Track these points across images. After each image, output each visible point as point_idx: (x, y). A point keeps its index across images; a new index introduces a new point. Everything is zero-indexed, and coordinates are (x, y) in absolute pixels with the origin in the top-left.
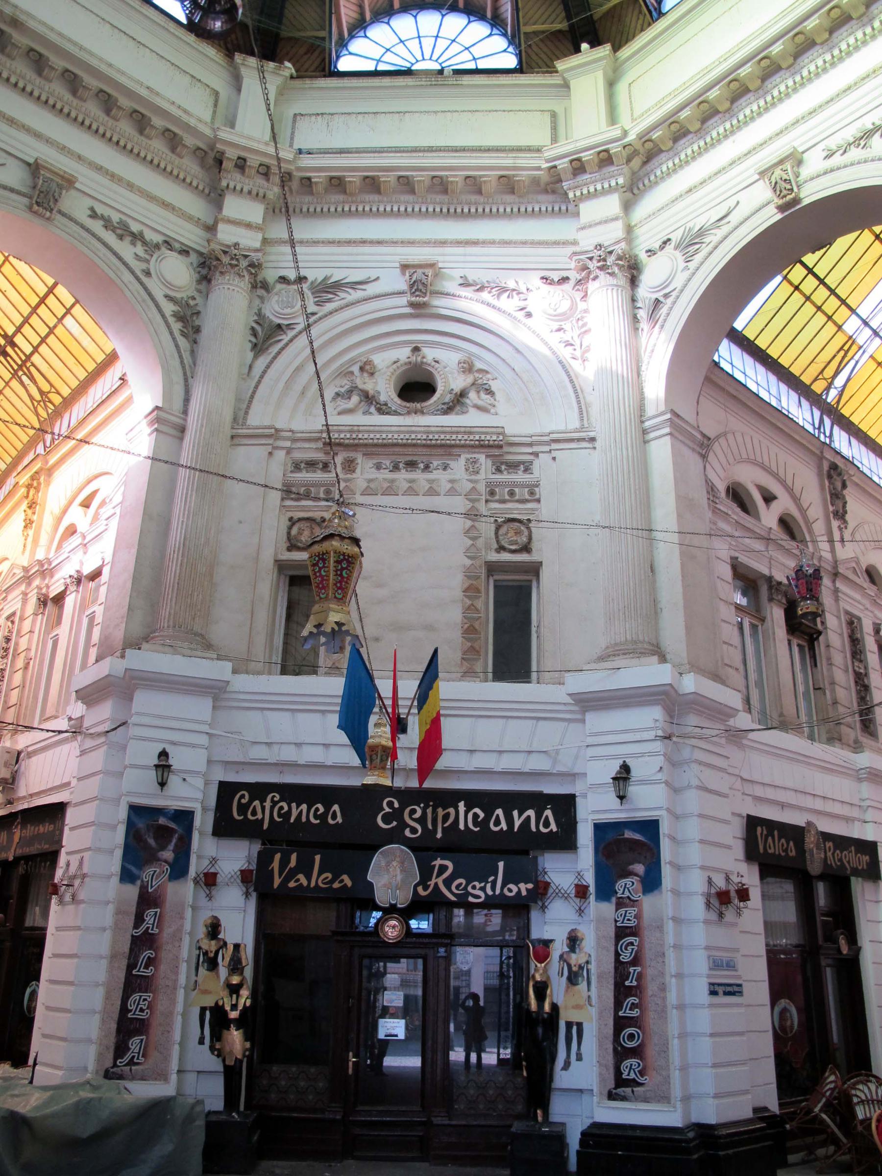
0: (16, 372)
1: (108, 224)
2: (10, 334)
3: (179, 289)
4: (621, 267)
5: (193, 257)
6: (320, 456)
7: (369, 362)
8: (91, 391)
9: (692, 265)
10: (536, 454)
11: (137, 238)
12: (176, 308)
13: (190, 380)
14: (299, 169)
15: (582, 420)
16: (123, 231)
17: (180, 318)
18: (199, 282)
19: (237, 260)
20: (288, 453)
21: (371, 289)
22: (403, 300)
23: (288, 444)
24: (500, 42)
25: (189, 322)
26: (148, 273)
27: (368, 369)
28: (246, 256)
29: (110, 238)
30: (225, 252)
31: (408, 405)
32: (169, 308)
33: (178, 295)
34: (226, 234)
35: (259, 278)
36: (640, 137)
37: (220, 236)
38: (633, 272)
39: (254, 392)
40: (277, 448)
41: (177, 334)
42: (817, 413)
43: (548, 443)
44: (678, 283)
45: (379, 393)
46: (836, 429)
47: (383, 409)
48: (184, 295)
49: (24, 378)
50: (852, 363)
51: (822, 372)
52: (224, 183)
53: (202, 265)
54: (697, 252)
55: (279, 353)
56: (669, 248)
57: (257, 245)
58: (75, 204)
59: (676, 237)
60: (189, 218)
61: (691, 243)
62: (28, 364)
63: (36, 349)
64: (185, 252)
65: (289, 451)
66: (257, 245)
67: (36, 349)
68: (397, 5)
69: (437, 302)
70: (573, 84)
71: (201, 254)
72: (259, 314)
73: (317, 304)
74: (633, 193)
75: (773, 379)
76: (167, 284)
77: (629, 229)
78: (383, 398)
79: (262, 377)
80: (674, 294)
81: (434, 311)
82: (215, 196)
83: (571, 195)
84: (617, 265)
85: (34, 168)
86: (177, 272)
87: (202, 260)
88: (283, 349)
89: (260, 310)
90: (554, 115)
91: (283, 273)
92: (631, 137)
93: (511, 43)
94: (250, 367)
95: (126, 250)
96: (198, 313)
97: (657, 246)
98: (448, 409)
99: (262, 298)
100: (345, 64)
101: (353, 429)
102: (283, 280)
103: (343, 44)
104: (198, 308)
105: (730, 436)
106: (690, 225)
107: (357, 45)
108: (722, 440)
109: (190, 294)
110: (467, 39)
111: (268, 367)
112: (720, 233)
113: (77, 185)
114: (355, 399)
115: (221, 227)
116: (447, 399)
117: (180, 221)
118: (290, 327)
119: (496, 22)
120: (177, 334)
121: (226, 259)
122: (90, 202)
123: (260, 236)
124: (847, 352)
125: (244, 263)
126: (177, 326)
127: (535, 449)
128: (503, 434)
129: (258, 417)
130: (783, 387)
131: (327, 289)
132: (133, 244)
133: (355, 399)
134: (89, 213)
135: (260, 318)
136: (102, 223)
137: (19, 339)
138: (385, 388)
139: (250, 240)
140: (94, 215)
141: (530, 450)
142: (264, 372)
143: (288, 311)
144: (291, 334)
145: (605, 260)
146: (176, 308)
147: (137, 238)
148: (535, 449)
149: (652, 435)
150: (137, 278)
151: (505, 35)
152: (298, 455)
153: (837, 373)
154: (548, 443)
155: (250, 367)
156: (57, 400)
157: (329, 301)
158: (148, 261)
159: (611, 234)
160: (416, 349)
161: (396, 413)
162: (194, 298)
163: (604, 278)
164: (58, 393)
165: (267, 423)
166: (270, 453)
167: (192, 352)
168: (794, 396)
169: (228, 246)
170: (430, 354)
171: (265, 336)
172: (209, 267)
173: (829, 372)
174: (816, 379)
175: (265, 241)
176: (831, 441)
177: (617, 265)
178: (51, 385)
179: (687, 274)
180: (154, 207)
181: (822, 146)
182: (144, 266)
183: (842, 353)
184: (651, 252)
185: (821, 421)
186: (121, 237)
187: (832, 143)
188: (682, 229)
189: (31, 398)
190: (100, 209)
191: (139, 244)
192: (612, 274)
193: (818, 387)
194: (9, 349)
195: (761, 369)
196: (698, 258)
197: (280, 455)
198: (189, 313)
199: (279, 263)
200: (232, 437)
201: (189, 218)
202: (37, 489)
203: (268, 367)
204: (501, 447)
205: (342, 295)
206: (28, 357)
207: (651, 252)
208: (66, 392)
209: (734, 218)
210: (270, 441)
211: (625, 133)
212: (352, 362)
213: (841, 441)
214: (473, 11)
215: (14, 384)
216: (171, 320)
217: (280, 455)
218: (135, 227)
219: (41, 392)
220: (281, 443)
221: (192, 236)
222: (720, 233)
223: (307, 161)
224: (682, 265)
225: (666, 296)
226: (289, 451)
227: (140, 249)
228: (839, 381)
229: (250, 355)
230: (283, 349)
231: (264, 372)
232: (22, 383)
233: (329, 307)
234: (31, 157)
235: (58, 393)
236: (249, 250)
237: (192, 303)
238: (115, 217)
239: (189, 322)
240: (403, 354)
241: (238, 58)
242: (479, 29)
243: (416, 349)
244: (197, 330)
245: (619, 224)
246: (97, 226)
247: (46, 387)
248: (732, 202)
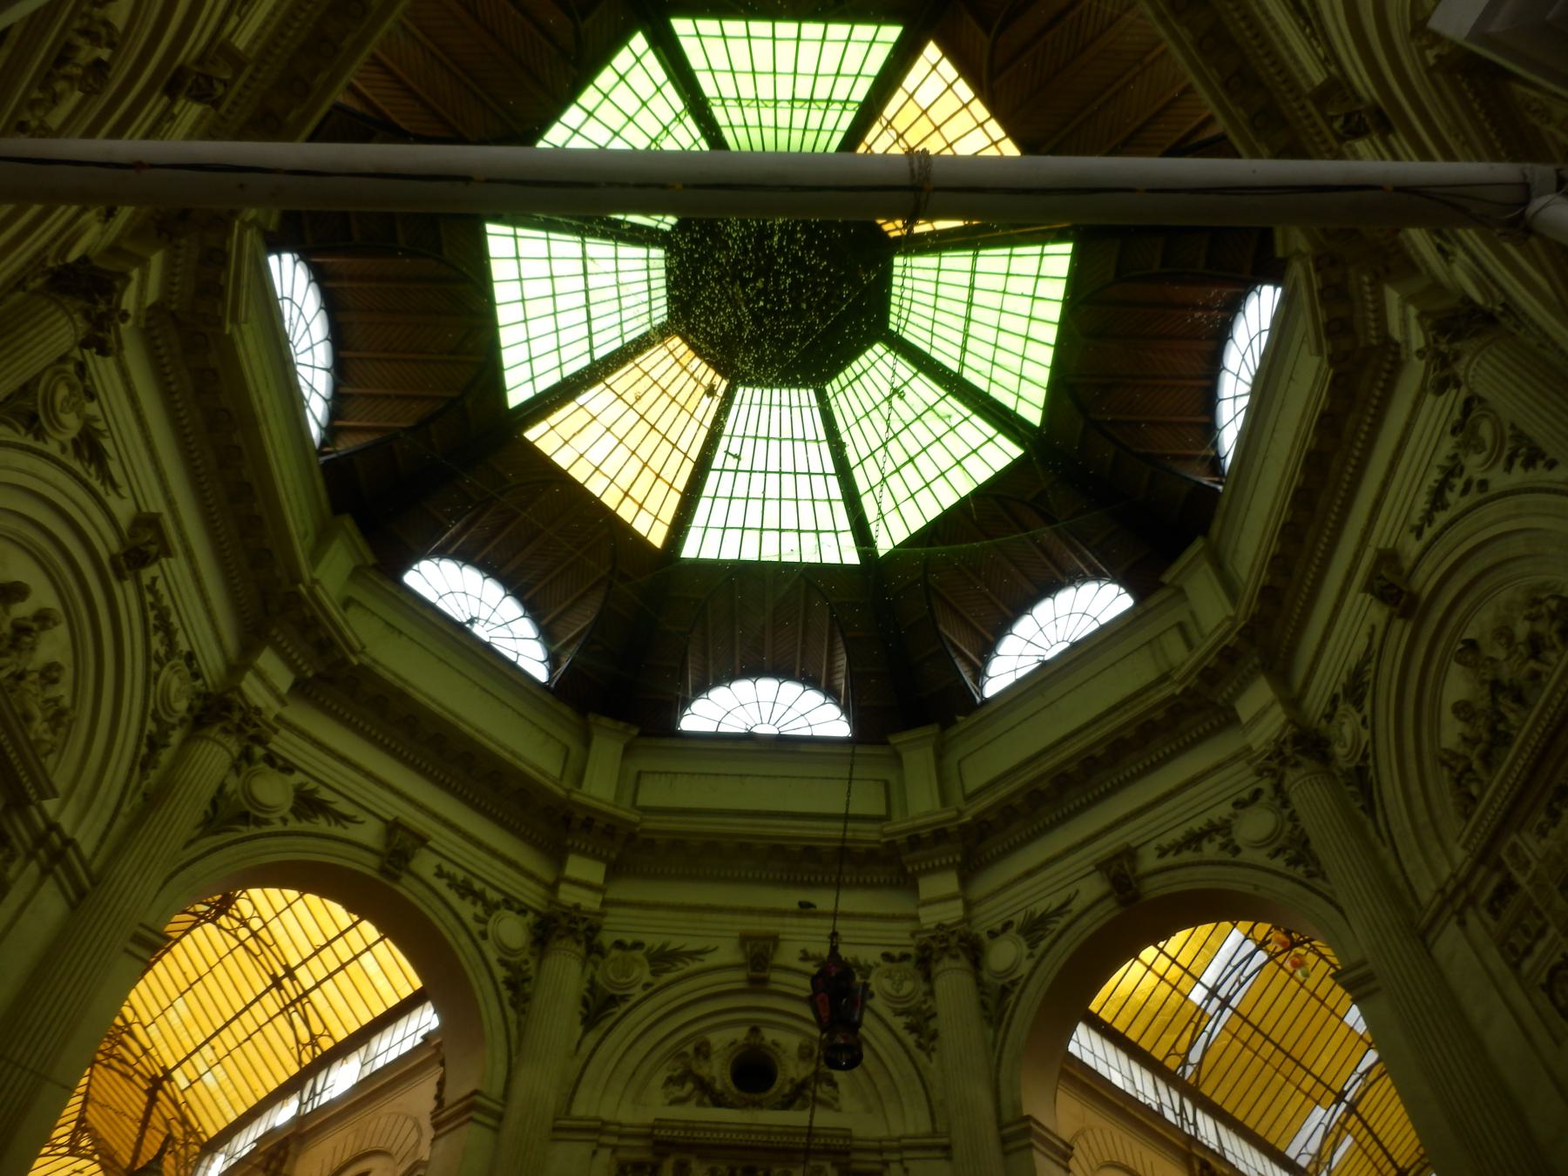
0: (286, 1007)
1: (453, 884)
2: (293, 965)
3: (514, 952)
4: (964, 949)
5: (530, 917)
6: (646, 1156)
7: (707, 1043)
8: (375, 1041)
9: (1038, 952)
10: (886, 1164)
11: (478, 896)
12: (508, 974)
13: (515, 1059)
14: (644, 831)
15: (933, 1120)
16: (465, 890)
17: (512, 985)
18: (534, 944)
20: (614, 1152)
21: (711, 960)
22: (741, 975)
23: (614, 1141)
24: (833, 711)
25: (519, 988)
26: (484, 935)
27: (703, 1051)
28: (585, 919)
29: (452, 897)
31: (746, 1095)
32: (501, 973)
33: (512, 959)
34: (569, 895)
35: (596, 941)
36: (975, 818)
38: (974, 952)
39: (582, 1074)
40: (601, 1145)
41: (506, 1002)
42: (1176, 1096)
43: (901, 1149)
44: (1025, 968)
45: (714, 1079)
46: (1199, 1114)
47: (718, 1101)
49: (295, 1016)
50: (1205, 1036)
51: (1173, 1046)
52: (569, 842)
53: (538, 926)
54: (1041, 938)
55: (610, 1029)
56: (1012, 931)
58: (425, 864)
59: (1019, 919)
60: (531, 876)
61: (1034, 928)
62: (305, 1000)
63: (318, 985)
64: (522, 912)
65: (615, 1149)
66: (597, 907)
67: (318, 985)
69: (775, 976)
70: (905, 756)
71: (537, 913)
72: (592, 982)
73: (655, 973)
74: (969, 870)
75: (1123, 1057)
76: (502, 947)
77: (969, 905)
78: (718, 1086)
79: (591, 1055)
80: (1022, 982)
81: (774, 987)
82: (557, 855)
83: (909, 869)
85: (393, 827)
86: (512, 930)
87: (538, 919)
88: (616, 1023)
89: (593, 977)
90: (887, 785)
91: (619, 937)
92: (967, 818)
93: (845, 710)
94: (579, 1044)
95: (467, 910)
96: (528, 980)
97: (998, 927)
98: (787, 1104)
99: (596, 965)
100: (688, 723)
101: (689, 1126)
102: (619, 945)
103: (687, 704)
104: (531, 973)
105: (1089, 1134)
106: (1032, 908)
107: (698, 706)
108: (1081, 1141)
109: (525, 956)
110: (802, 706)
111: (598, 1044)
112: (1063, 921)
113: (430, 843)
114: (689, 1086)
115: (563, 887)
116: (787, 1089)
117: (523, 879)
118: (624, 998)
119: (830, 692)
120: (506, 1002)
121: (564, 922)
122: (436, 860)
123: (600, 898)
124: (1197, 1025)
125: (582, 927)
126: (507, 994)
127: (886, 1156)
128: (850, 1137)
129: (582, 1108)
130: (1135, 1067)
131: (663, 959)
132: (474, 903)
133: (689, 1086)
135: (593, 986)
136: (445, 881)
137: (301, 973)
138: (718, 1071)
139: (590, 901)
141: (879, 1158)
142: (594, 1050)
143: (623, 980)
144: (624, 1007)
145: (947, 940)
146: (508, 974)
147: (478, 896)
148: (886, 1156)
149: (1012, 1146)
150: (474, 941)
151: (837, 704)
152: (622, 1155)
153: (1192, 1045)
154: (901, 1149)
155: (579, 1044)
156: (327, 1044)
157: (667, 971)
158: (485, 922)
159: (952, 913)
160: (755, 1030)
161: (731, 1106)
162: (526, 962)
163: (947, 962)
164: (331, 1036)
165: (592, 1114)
166: (595, 1153)
167: (519, 1023)
168: (1148, 1077)
170: (769, 1035)
171: (599, 1007)
172: (549, 928)
173: (1182, 1046)
174: (1168, 1055)
175: (604, 903)
176: (1196, 1129)
178: (326, 1027)
179: (1031, 963)
180: (499, 865)
181: (1154, 844)
182: (481, 927)
183: (1192, 1026)
184: (993, 934)
185: (1182, 1107)
186: (463, 896)
187: (1166, 841)
188: (1022, 914)
189: (298, 1041)
190: (447, 867)
191: (480, 904)
193: (1172, 1063)
194: (281, 973)
195: (1110, 1048)
196: (1043, 944)
197: (605, 1155)
199: (618, 926)
200: (555, 1129)
201: (531, 876)
202: (282, 1162)
203: (598, 1044)
204: (847, 1153)
205: (680, 965)
206: (306, 993)
207: (993, 934)
208: (341, 1035)
209: (1076, 906)
210: (596, 1137)
211: (960, 813)
212: (686, 1040)
213: (1208, 1130)
214: (810, 681)
215: (281, 1022)
216: (502, 987)
217: (605, 1155)
218: (478, 885)
219: (312, 1036)
220: (605, 1139)
221: (532, 895)
222: (1063, 921)
223: (650, 824)
224: (1026, 951)
225: (1014, 983)
226: (615, 1149)
227: (479, 910)
228: (1195, 1056)
229: (579, 1030)
230: (616, 1023)
231: (594, 1050)
232: (292, 1024)
233: (666, 977)
235: (331, 1036)
236: (589, 912)
237: (525, 967)
238: (460, 875)
239: (519, 988)
240: (741, 1034)
241: (591, 717)
242: (814, 697)
243: (755, 1030)
244: (527, 999)
245: (959, 903)
246: (441, 885)
247: (317, 1028)
248: (1071, 890)
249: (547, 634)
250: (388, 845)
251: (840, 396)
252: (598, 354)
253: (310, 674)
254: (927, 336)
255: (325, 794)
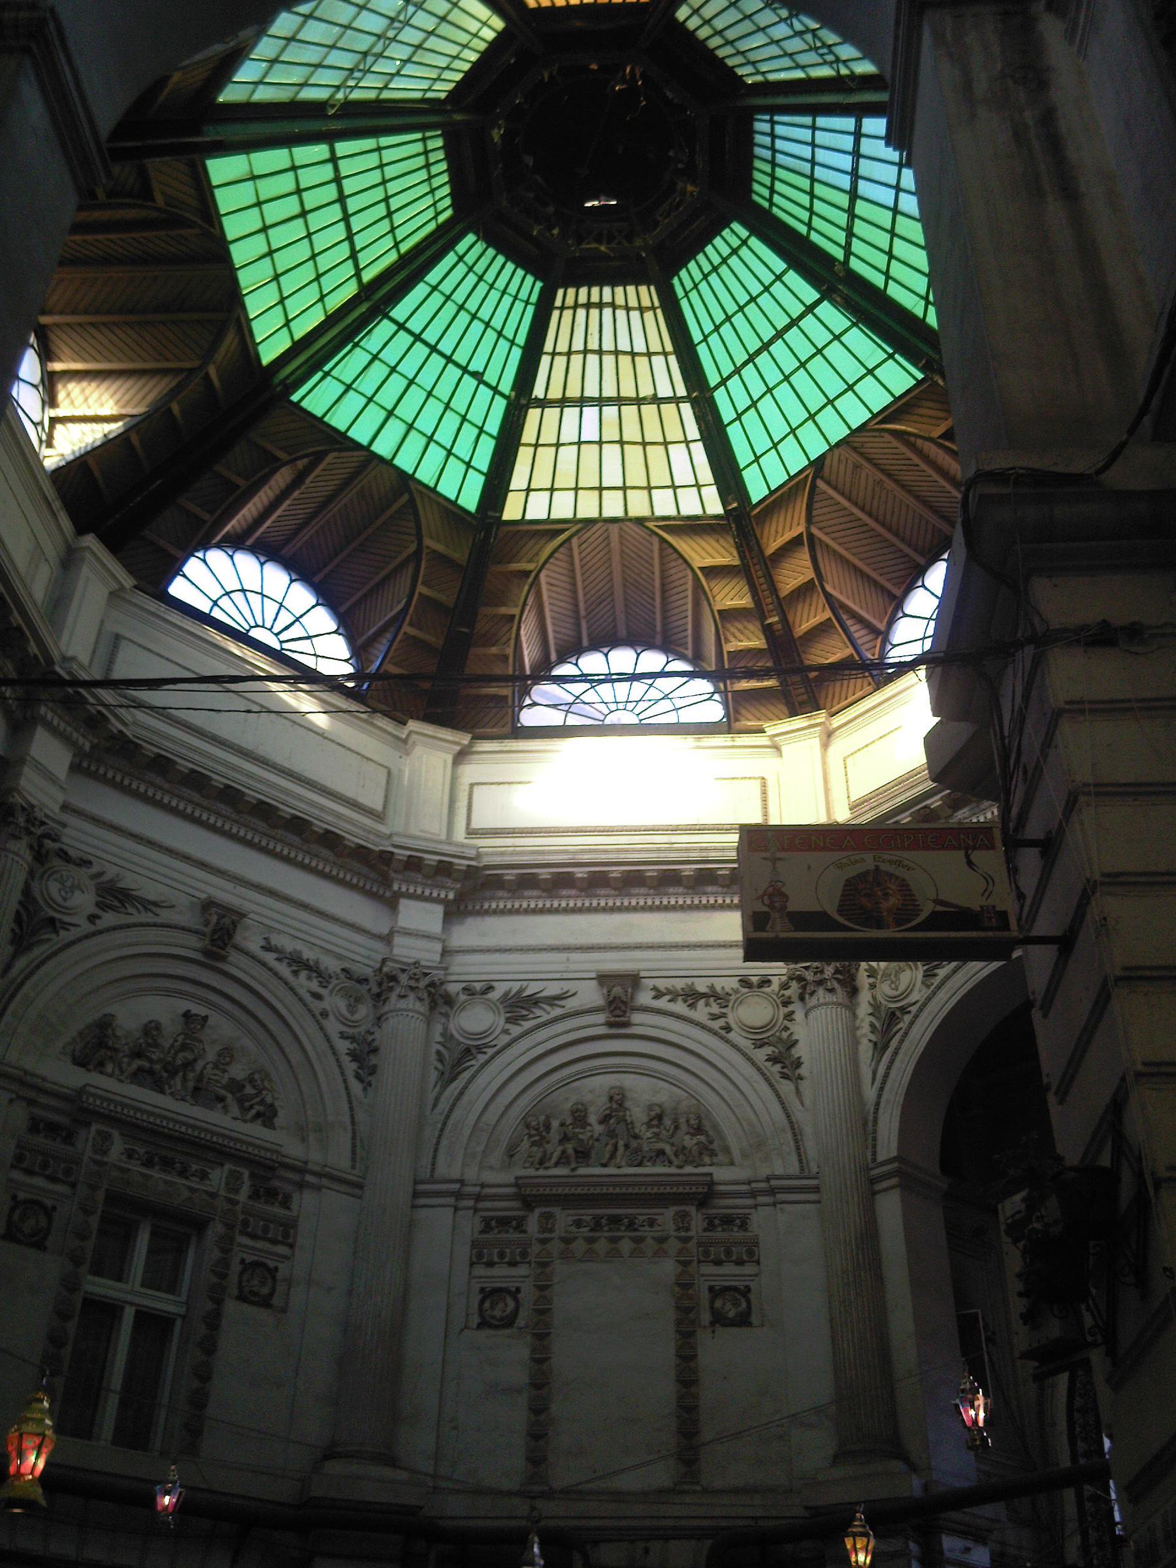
19: (417, 980)
28: (426, 974)
30: (403, 971)
37: (396, 951)
48: (362, 1029)
57: (437, 958)
68: (585, 643)
82: (392, 904)
84: (836, 979)
100: (529, 718)
115: (398, 940)
134: (263, 943)
139: (428, 953)
140: (268, 948)
169: (409, 964)
175: (445, 952)
177: (836, 979)
192: (832, 991)
198: (367, 1049)
226: (476, 1210)
234: (203, 892)
236: (429, 967)
246: (269, 958)
249: (348, 626)
250: (207, 924)
251: (693, 295)
252: (367, 276)
253: (87, 747)
254: (805, 215)
255: (129, 881)
